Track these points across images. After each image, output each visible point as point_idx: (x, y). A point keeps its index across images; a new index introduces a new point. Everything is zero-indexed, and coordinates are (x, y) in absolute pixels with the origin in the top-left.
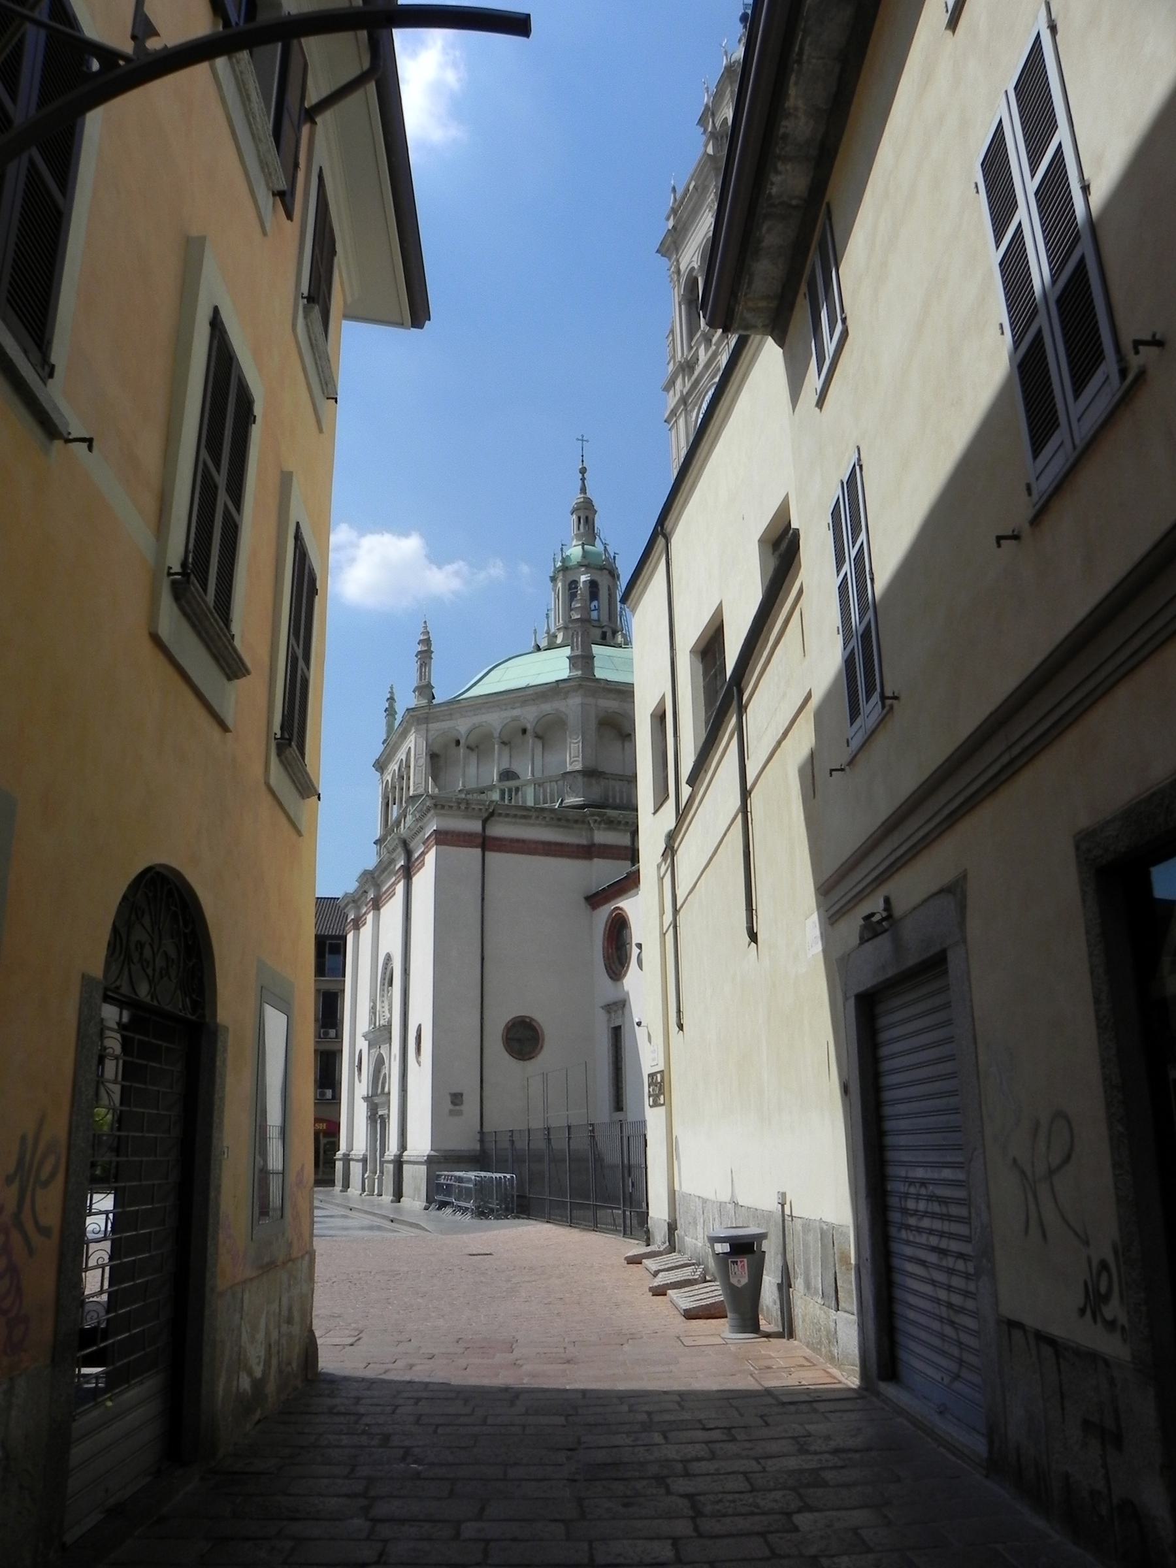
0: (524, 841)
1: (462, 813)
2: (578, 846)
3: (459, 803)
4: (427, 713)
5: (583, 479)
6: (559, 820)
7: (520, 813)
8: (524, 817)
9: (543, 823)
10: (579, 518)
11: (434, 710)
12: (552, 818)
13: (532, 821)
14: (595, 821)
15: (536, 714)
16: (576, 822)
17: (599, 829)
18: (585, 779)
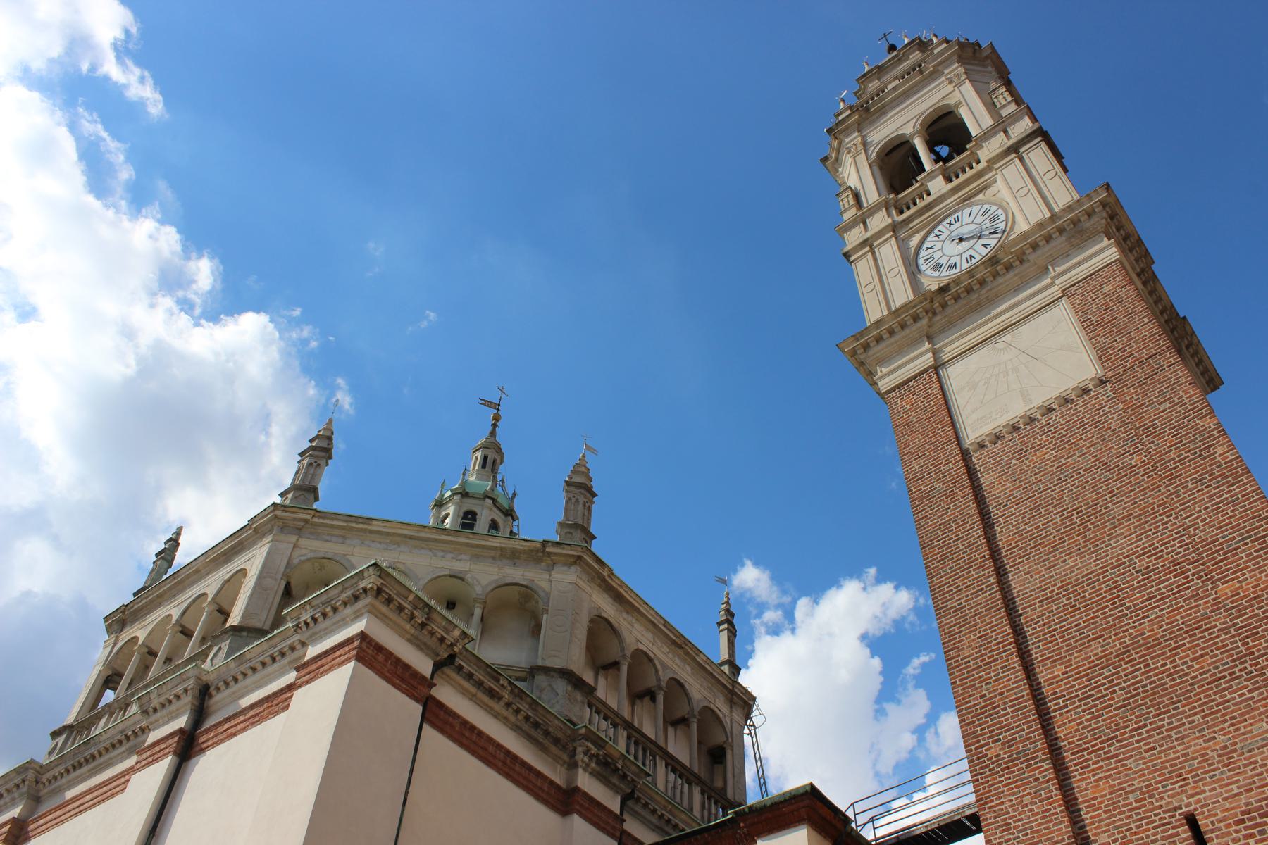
0: (480, 734)
1: (412, 631)
2: (552, 783)
3: (416, 608)
4: (306, 521)
5: (495, 426)
6: (536, 725)
7: (489, 683)
8: (492, 694)
9: (512, 718)
10: (485, 458)
11: (321, 521)
12: (527, 718)
13: (498, 707)
14: (586, 752)
15: (496, 577)
16: (556, 741)
17: (585, 770)
18: (569, 688)
